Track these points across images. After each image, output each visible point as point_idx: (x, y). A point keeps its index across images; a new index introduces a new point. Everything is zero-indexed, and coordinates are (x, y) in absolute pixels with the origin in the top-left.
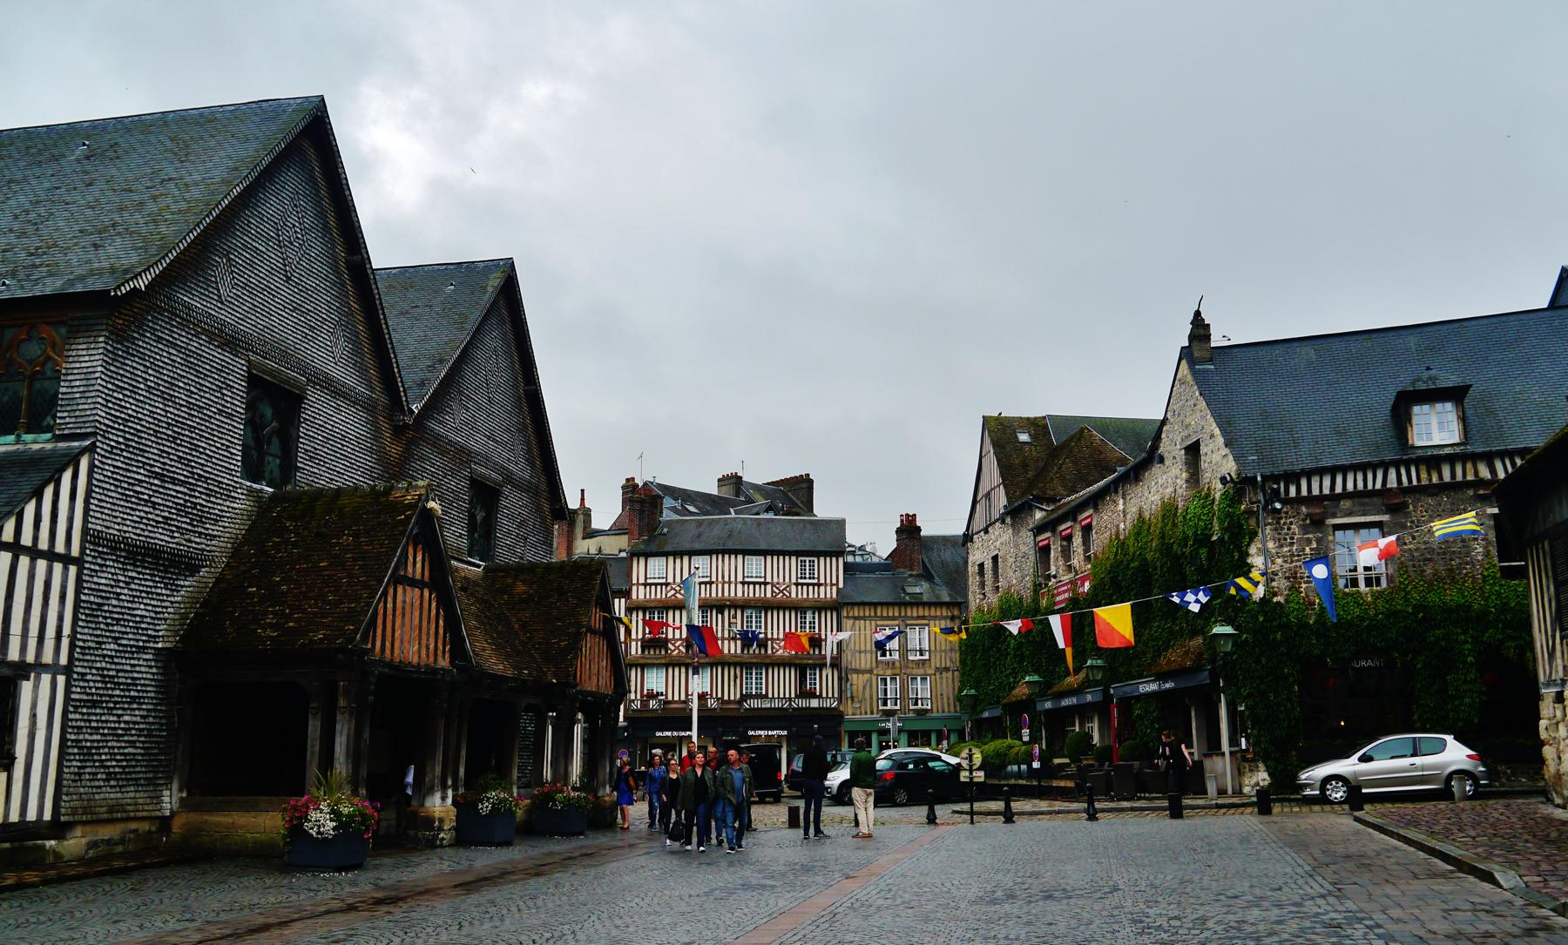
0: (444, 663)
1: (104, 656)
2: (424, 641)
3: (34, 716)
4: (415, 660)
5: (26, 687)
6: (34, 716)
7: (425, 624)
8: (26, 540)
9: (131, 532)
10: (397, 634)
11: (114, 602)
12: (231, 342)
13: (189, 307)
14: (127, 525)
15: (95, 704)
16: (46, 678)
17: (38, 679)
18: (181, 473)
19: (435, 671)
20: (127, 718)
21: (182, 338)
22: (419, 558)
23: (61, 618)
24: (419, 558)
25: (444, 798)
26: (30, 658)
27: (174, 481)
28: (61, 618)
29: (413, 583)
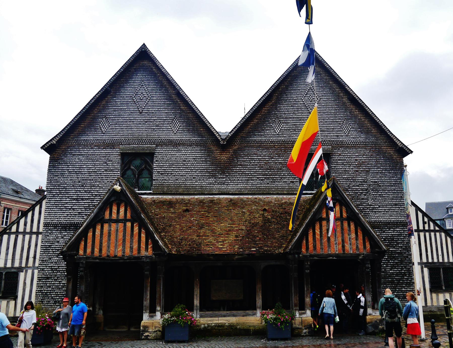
0: (147, 252)
1: (52, 262)
2: (128, 245)
3: (25, 283)
4: (120, 254)
5: (22, 275)
6: (25, 283)
7: (128, 237)
8: (21, 229)
9: (63, 220)
10: (105, 244)
11: (56, 244)
12: (111, 145)
13: (86, 140)
14: (62, 218)
15: (48, 278)
16: (30, 272)
17: (26, 271)
18: (86, 196)
19: (138, 258)
20: (63, 282)
21: (85, 151)
22: (122, 210)
23: (35, 252)
24: (122, 210)
25: (151, 317)
26: (23, 265)
27: (82, 199)
28: (35, 252)
29: (117, 221)
